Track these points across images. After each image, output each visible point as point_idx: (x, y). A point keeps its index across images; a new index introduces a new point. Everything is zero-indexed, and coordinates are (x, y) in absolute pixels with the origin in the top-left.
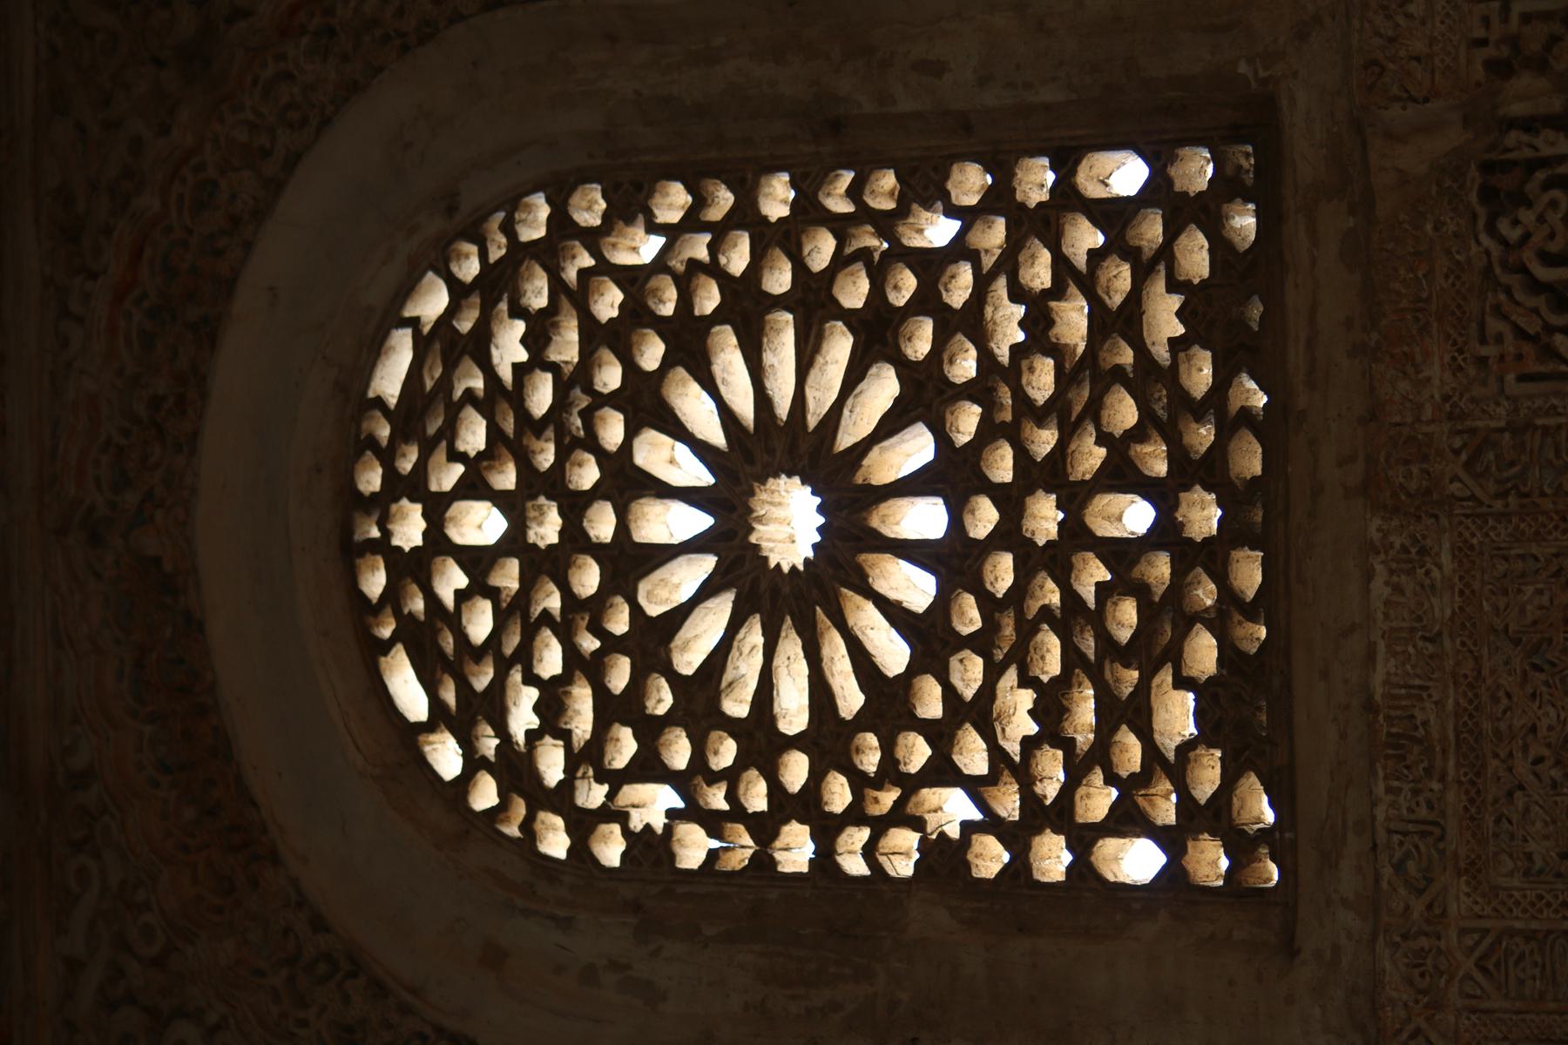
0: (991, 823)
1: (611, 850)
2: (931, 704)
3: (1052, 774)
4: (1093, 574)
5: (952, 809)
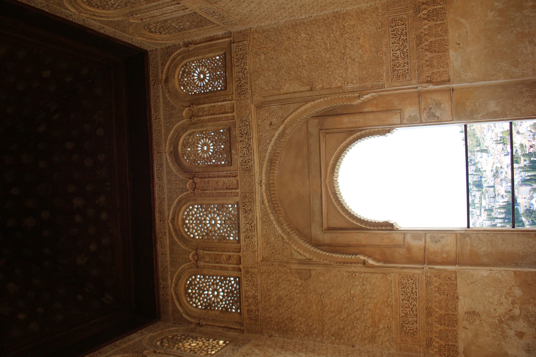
5: (214, 161)
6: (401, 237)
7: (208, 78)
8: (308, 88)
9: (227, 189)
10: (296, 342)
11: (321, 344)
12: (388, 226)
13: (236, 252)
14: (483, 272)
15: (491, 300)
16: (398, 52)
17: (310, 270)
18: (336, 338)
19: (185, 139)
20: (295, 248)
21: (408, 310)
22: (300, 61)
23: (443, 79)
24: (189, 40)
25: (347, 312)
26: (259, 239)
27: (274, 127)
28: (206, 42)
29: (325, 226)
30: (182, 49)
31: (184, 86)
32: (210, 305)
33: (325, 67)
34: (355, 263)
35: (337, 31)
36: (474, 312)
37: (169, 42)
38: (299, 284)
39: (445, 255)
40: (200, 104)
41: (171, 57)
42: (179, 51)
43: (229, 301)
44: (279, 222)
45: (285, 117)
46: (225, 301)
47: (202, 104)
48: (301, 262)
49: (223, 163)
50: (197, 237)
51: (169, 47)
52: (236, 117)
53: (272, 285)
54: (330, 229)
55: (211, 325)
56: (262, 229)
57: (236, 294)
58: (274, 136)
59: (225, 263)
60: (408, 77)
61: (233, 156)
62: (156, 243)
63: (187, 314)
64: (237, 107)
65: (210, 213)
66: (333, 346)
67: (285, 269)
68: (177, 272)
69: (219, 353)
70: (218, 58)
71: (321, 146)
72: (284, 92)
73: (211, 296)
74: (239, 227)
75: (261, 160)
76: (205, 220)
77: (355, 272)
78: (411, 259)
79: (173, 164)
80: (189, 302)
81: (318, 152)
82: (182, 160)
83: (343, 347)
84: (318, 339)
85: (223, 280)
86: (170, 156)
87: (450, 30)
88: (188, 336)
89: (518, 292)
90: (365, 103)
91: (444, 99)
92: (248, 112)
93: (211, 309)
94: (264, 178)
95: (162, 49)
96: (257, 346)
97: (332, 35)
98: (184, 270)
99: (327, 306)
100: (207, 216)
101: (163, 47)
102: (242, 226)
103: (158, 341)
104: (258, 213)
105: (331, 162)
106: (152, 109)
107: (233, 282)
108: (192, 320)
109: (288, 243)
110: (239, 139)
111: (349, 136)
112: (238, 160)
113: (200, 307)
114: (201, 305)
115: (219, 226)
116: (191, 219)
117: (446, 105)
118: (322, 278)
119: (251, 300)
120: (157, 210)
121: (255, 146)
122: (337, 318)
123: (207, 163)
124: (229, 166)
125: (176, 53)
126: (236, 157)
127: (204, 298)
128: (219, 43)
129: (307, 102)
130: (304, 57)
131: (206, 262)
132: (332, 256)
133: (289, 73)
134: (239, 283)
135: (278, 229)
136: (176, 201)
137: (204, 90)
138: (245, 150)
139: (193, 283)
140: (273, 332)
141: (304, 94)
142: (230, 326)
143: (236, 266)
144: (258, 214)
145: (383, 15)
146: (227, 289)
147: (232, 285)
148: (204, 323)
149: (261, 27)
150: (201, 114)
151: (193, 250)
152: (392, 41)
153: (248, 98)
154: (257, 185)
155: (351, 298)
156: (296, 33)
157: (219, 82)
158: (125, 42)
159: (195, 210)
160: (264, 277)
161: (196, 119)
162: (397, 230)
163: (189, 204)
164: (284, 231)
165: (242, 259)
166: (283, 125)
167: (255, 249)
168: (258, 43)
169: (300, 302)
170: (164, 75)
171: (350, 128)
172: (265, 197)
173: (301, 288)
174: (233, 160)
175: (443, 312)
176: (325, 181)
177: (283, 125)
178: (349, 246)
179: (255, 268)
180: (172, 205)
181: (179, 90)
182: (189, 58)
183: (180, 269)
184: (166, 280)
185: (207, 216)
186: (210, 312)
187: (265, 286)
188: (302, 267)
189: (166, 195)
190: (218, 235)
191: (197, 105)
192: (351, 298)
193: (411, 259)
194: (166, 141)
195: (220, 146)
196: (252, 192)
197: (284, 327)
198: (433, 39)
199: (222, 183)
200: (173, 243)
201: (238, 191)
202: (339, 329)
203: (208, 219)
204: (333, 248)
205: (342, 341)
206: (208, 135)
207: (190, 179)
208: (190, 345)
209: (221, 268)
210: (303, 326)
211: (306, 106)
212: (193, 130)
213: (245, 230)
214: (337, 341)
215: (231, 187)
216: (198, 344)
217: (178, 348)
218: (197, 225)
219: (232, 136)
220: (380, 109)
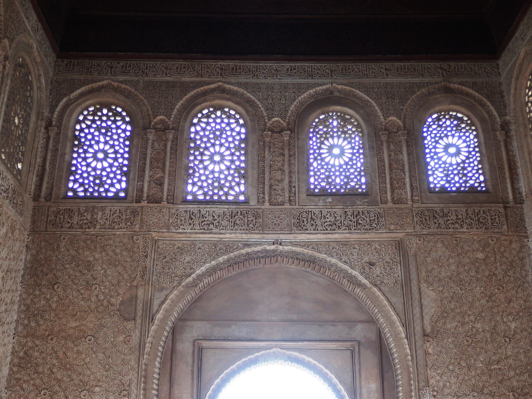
0: (314, 168)
1: (311, 135)
2: (323, 163)
3: (318, 174)
4: (333, 178)
5: (315, 164)
8: (428, 330)
9: (271, 186)
10: (17, 291)
11: (12, 334)
13: (168, 195)
17: (134, 319)
18: (21, 358)
19: (352, 117)
20: (172, 296)
24: (513, 133)
25: (65, 378)
26: (188, 235)
29: (205, 344)
30: (498, 119)
32: (81, 145)
33: (461, 359)
35: (518, 381)
38: (113, 300)
40: (408, 146)
41: (485, 100)
42: (495, 113)
43: (87, 178)
45: (382, 288)
47: (408, 150)
48: (148, 304)
51: (503, 97)
52: (384, 206)
55: (47, 145)
56: (204, 242)
57: (98, 191)
58: (352, 268)
59: (150, 177)
61: (322, 198)
62: (185, 59)
64: (401, 209)
65: (232, 154)
66: (9, 354)
67: (138, 278)
70: (482, 178)
71: (334, 343)
72: (422, 289)
75: (316, 246)
76: (221, 145)
79: (313, 96)
80: (87, 109)
81: (323, 337)
82: (319, 111)
84: (20, 328)
85: (121, 170)
86: (326, 90)
92: (392, 227)
93: (76, 146)
94: (286, 248)
95: (500, 84)
96: (12, 229)
97: (512, 373)
99: (76, 346)
100: (228, 148)
101: (504, 87)
102: (210, 208)
103: (23, 59)
104: (229, 236)
106: (402, 64)
107: (118, 186)
108: (56, 113)
109: (180, 284)
110: (350, 210)
111: (347, 390)
112: (316, 207)
113: (78, 127)
114: (82, 130)
115: (211, 167)
116: (222, 122)
118: (121, 338)
119: (89, 217)
120: (238, 63)
123: (313, 154)
125: (492, 108)
126: (321, 203)
127: (92, 134)
128: (504, 182)
130: (479, 326)
131: (153, 144)
132: (157, 356)
133: (452, 298)
135: (203, 269)
136: (253, 98)
137: (430, 153)
138: (332, 219)
139: (118, 118)
141: (418, 321)
142: (46, 179)
143: (145, 195)
144: (228, 236)
147: (112, 185)
148: (52, 134)
150: (392, 147)
153: (414, 228)
154: (275, 237)
155: (88, 387)
156: (518, 313)
157: (442, 180)
158: (517, 26)
160: (126, 240)
161: (384, 138)
163: (248, 119)
164: (200, 277)
165: (156, 205)
167: (172, 228)
168: (502, 249)
169: (83, 299)
170: (456, 86)
171: (361, 393)
173: (105, 303)
174: (316, 199)
176: (276, 346)
179: (141, 227)
182: (483, 131)
184: (124, 73)
186: (69, 145)
187: (111, 242)
189: (263, 81)
190: (195, 165)
191: (407, 142)
192: (88, 387)
194: (350, 85)
196: (263, 228)
197: (42, 271)
199: (279, 178)
201: (267, 205)
202: (37, 365)
204: (171, 355)
205: (15, 369)
206: (359, 157)
207: (288, 124)
210: (43, 302)
211: (398, 324)
213: (203, 212)
214: (16, 361)
215: (273, 193)
219: (354, 198)
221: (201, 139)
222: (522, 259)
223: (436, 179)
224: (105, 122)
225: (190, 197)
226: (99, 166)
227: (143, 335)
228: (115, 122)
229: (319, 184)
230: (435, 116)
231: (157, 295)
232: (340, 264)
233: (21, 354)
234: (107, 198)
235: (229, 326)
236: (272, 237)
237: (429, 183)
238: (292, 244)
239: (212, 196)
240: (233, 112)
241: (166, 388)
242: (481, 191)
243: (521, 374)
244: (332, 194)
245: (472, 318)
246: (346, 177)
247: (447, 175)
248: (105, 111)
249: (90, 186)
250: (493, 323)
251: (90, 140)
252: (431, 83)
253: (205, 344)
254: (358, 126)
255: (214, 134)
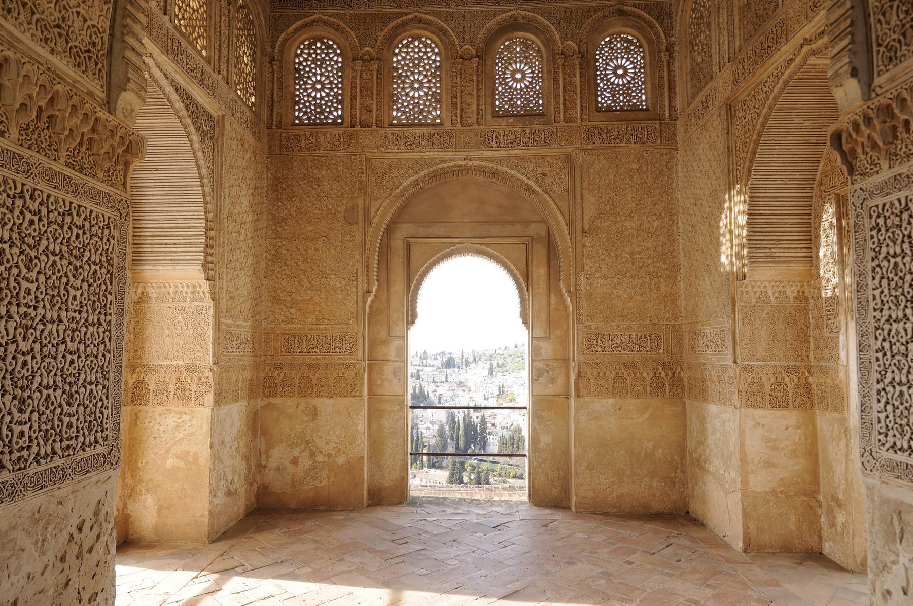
5: (500, 89)
6: (399, 334)
7: (616, 82)
8: (587, 228)
9: (462, 110)
12: (411, 318)
14: (362, 425)
15: (331, 433)
16: (618, 341)
17: (357, 223)
19: (533, 42)
21: (315, 342)
22: (623, 218)
23: (582, 389)
24: (676, 54)
27: (540, 179)
28: (669, 79)
29: (412, 241)
31: (610, 42)
32: (301, 77)
34: (368, 280)
36: (316, 415)
37: (678, 20)
38: (339, 209)
39: (379, 382)
40: (581, 69)
42: (662, 35)
44: (417, 182)
46: (308, 101)
48: (367, 211)
49: (497, 103)
50: (395, 59)
51: (671, 18)
52: (557, 124)
53: (335, 171)
54: (408, 247)
56: (408, 159)
60: (587, 351)
63: (285, 40)
65: (429, 81)
68: (344, 25)
69: (240, 103)
73: (314, 79)
74: (410, 125)
76: (420, 73)
77: (356, 280)
78: (374, 344)
80: (302, 43)
82: (504, 38)
83: (263, 264)
84: (270, 233)
85: (337, 99)
86: (511, 17)
87: (639, 400)
88: (255, 46)
89: (341, 460)
90: (562, 295)
91: (558, 387)
94: (475, 163)
96: (254, 153)
97: (651, 261)
98: (347, 37)
100: (426, 76)
101: (673, 8)
102: (412, 130)
104: (428, 154)
105: (491, 251)
109: (390, 194)
111: (521, 274)
112: (501, 126)
113: (297, 61)
114: (300, 63)
115: (411, 94)
117: (551, 390)
118: (348, 238)
119: (314, 141)
121: (516, 152)
122: (299, 257)
123: (498, 79)
124: (493, 112)
125: (660, 30)
126: (504, 123)
127: (309, 66)
129: (568, 225)
130: (628, 224)
131: (361, 74)
134: (335, 123)
137: (599, 75)
138: (513, 137)
140: (273, 172)
142: (275, 108)
143: (358, 121)
144: (427, 154)
145: (667, 326)
146: (326, 105)
148: (275, 68)
149: (677, 165)
150: (567, 70)
151: (378, 53)
152: (633, 335)
154: (466, 153)
157: (609, 100)
159: (433, 58)
161: (560, 62)
162: (408, 329)
164: (406, 189)
166: (541, 192)
168: (654, 160)
170: (630, 8)
172: (450, 164)
173: (333, 211)
175: (314, 381)
177: (541, 192)
178: (388, 270)
180: (440, 18)
181: (605, 34)
183: (349, 30)
185: (426, 76)
186: (292, 76)
188: (361, 212)
189: (455, 9)
193: (374, 344)
194: (533, 10)
195: (520, 99)
196: (456, 147)
198: (629, 381)
200: (386, 19)
203: (421, 77)
204: (385, 251)
207: (477, 51)
208: (245, 53)
209: (354, 98)
211: (563, 223)
212: (545, 56)
214: (270, 257)
216: (247, 65)
217: (238, 37)
218: (412, 60)
219: (532, 118)
220: (552, 313)
221: (402, 68)
222: (669, 169)
223: (604, 99)
224: (320, 54)
225: (395, 122)
226: (318, 96)
227: (365, 234)
228: (328, 54)
229: (503, 105)
230: (607, 39)
231: (373, 204)
232: (518, 175)
233: (273, 252)
234: (327, 124)
235: (430, 227)
236: (463, 154)
237: (598, 103)
238: (480, 159)
239: (413, 120)
240: (429, 42)
241: (384, 274)
242: (642, 110)
243: (658, 261)
244: (513, 115)
245: (623, 218)
246: (526, 99)
247: (613, 96)
248: (318, 45)
249: (312, 114)
250: (639, 222)
251: (308, 72)
252: (606, 6)
253: (412, 241)
254: (539, 51)
255: (413, 63)
